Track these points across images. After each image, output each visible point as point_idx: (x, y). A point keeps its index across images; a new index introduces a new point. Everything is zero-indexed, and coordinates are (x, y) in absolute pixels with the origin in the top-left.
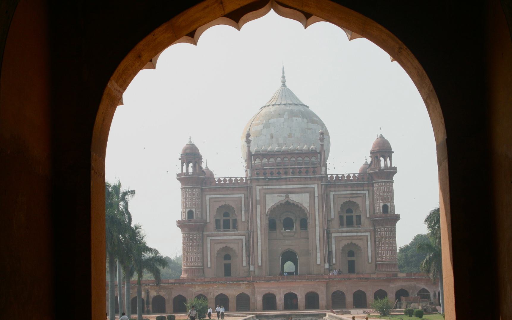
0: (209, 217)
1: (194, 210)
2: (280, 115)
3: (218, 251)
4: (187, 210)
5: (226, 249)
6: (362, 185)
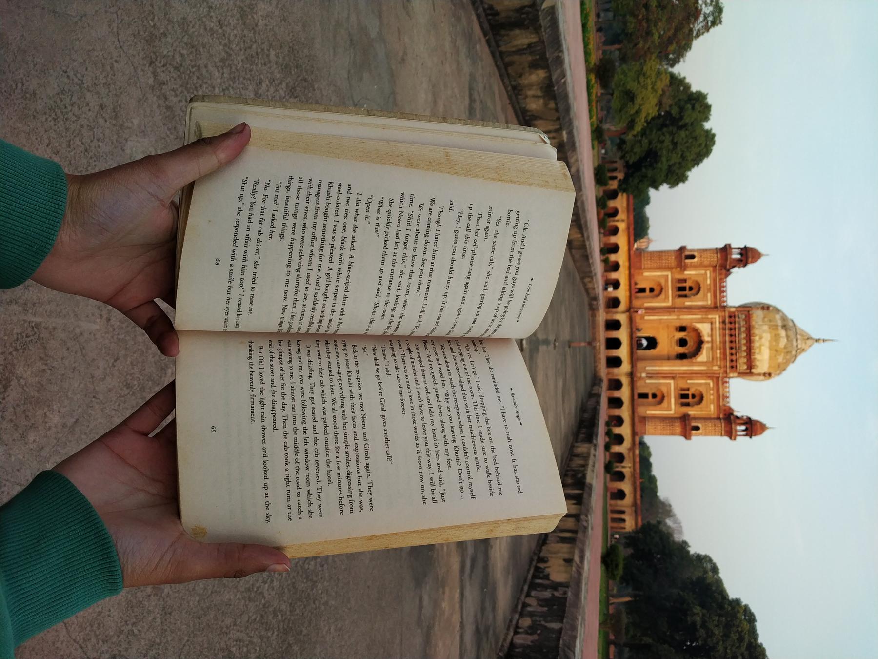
1: (696, 260)
4: (696, 254)
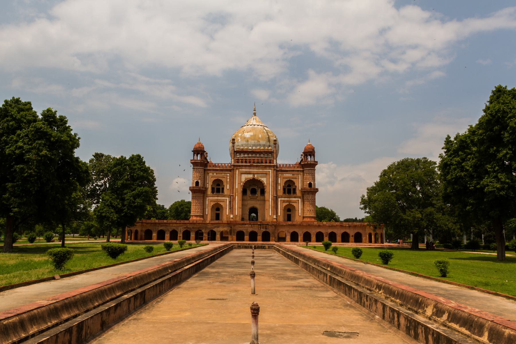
0: (209, 186)
1: (199, 181)
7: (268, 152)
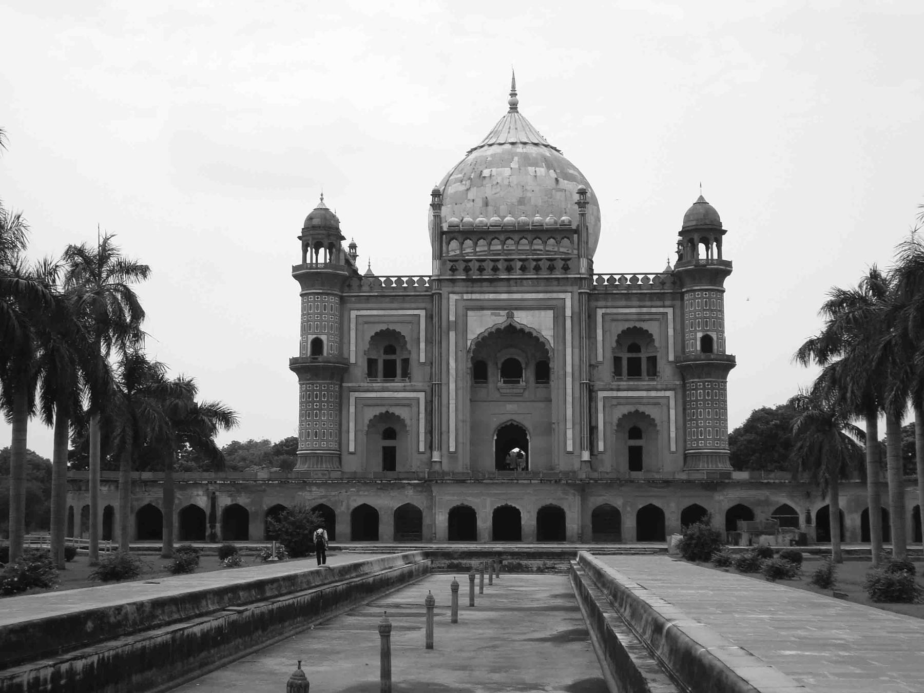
1: (324, 338)
2: (503, 161)
3: (370, 421)
4: (311, 337)
5: (387, 417)
6: (661, 296)
7: (556, 231)
